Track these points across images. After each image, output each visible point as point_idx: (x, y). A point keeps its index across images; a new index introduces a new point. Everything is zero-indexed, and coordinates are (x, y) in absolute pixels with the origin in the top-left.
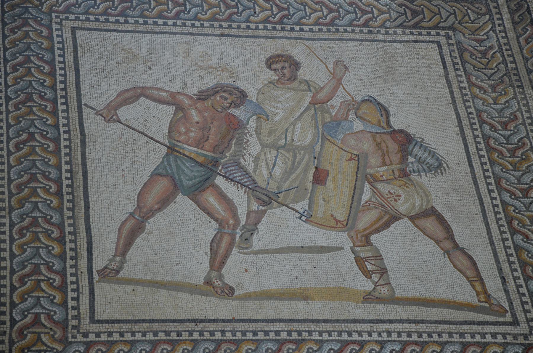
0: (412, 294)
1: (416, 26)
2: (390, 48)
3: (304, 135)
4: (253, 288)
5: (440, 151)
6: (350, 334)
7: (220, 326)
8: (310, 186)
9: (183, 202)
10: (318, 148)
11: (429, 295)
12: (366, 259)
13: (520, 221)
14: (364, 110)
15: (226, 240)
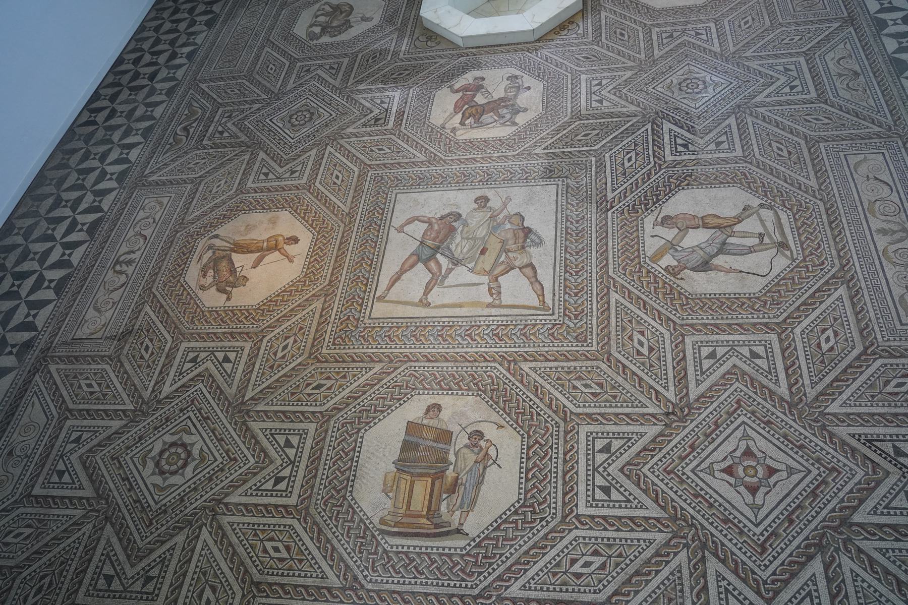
1: (550, 177)
2: (534, 189)
3: (482, 232)
4: (439, 303)
9: (420, 266)
11: (517, 304)
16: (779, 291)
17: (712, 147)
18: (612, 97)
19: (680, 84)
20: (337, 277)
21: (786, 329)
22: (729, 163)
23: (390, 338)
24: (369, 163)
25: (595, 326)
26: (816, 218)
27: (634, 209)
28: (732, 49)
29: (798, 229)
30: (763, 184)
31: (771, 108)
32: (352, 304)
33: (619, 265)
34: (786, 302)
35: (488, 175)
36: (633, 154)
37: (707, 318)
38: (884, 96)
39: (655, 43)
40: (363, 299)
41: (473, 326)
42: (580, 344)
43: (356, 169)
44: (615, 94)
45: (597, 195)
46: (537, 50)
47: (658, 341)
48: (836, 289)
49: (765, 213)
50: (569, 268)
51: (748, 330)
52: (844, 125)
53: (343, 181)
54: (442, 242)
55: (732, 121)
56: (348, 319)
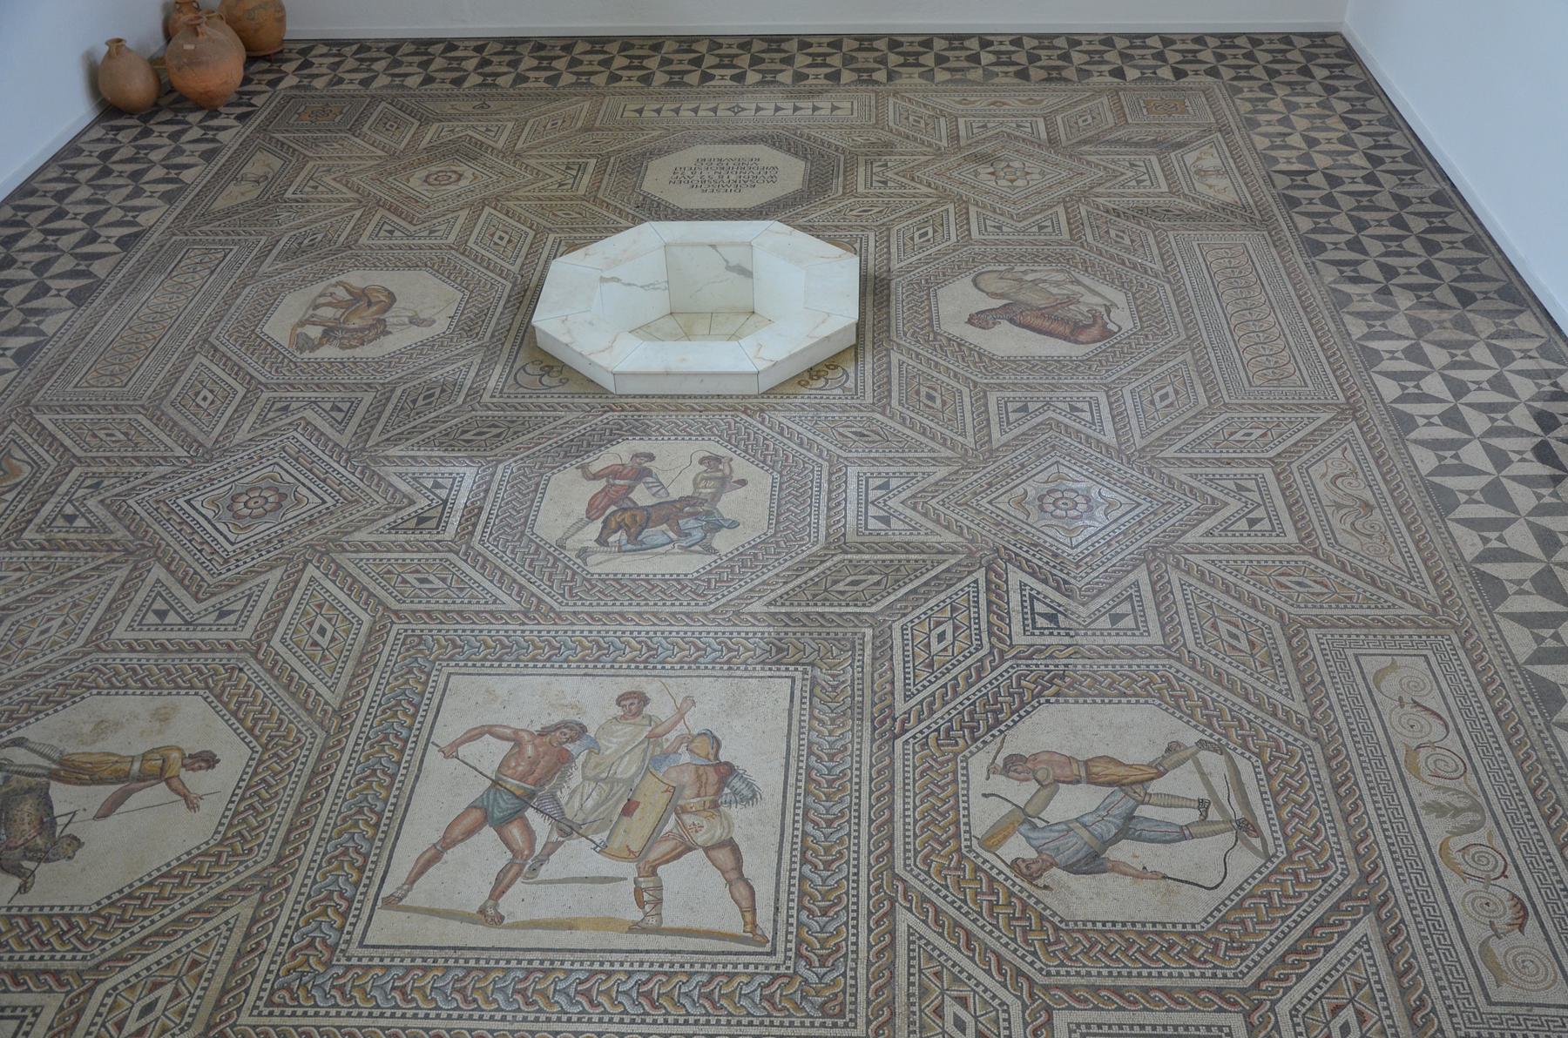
0: (679, 924)
1: (777, 662)
2: (744, 683)
3: (628, 768)
4: (522, 916)
5: (759, 783)
6: (602, 964)
7: (476, 954)
8: (615, 818)
9: (488, 833)
10: (637, 781)
11: (695, 926)
12: (645, 890)
13: (815, 851)
14: (697, 743)
15: (515, 869)
16: (1242, 922)
17: (1104, 622)
18: (909, 512)
19: (1041, 498)
20: (297, 849)
21: (1261, 1002)
22: (1136, 657)
23: (404, 994)
24: (394, 605)
25: (862, 983)
26: (1307, 774)
27: (948, 737)
28: (1140, 443)
29: (1275, 795)
30: (1204, 701)
31: (1213, 557)
32: (324, 912)
33: (916, 853)
34: (1258, 945)
35: (649, 649)
36: (948, 628)
37: (1097, 973)
38: (1419, 550)
39: (994, 419)
40: (350, 901)
41: (597, 972)
42: (829, 1022)
43: (365, 617)
44: (914, 509)
45: (874, 704)
46: (762, 411)
47: (996, 1021)
48: (1355, 923)
49: (1207, 757)
50: (810, 854)
51: (1184, 1003)
52: (1350, 598)
53: (333, 639)
54: (540, 783)
55: (1141, 575)
56: (311, 945)
